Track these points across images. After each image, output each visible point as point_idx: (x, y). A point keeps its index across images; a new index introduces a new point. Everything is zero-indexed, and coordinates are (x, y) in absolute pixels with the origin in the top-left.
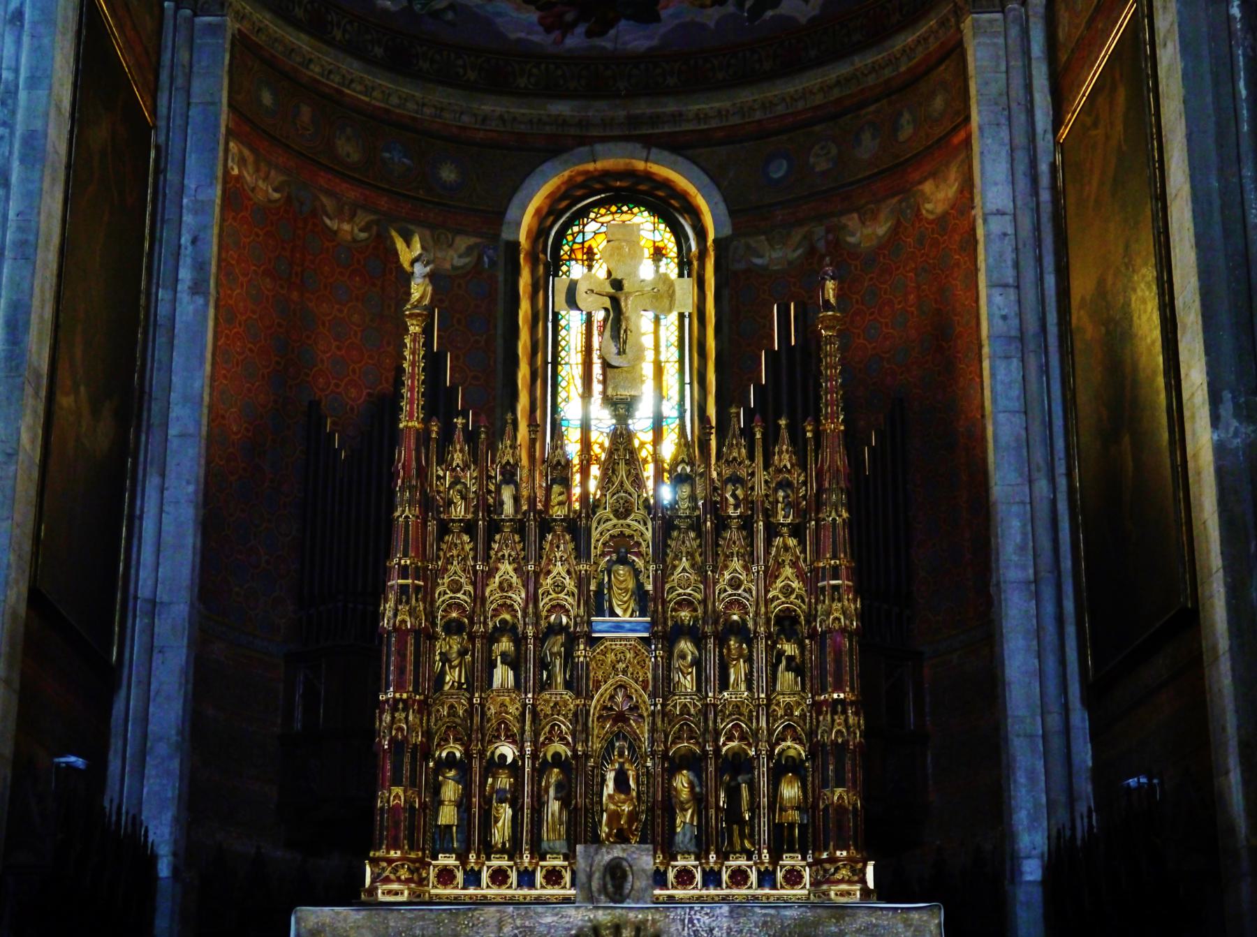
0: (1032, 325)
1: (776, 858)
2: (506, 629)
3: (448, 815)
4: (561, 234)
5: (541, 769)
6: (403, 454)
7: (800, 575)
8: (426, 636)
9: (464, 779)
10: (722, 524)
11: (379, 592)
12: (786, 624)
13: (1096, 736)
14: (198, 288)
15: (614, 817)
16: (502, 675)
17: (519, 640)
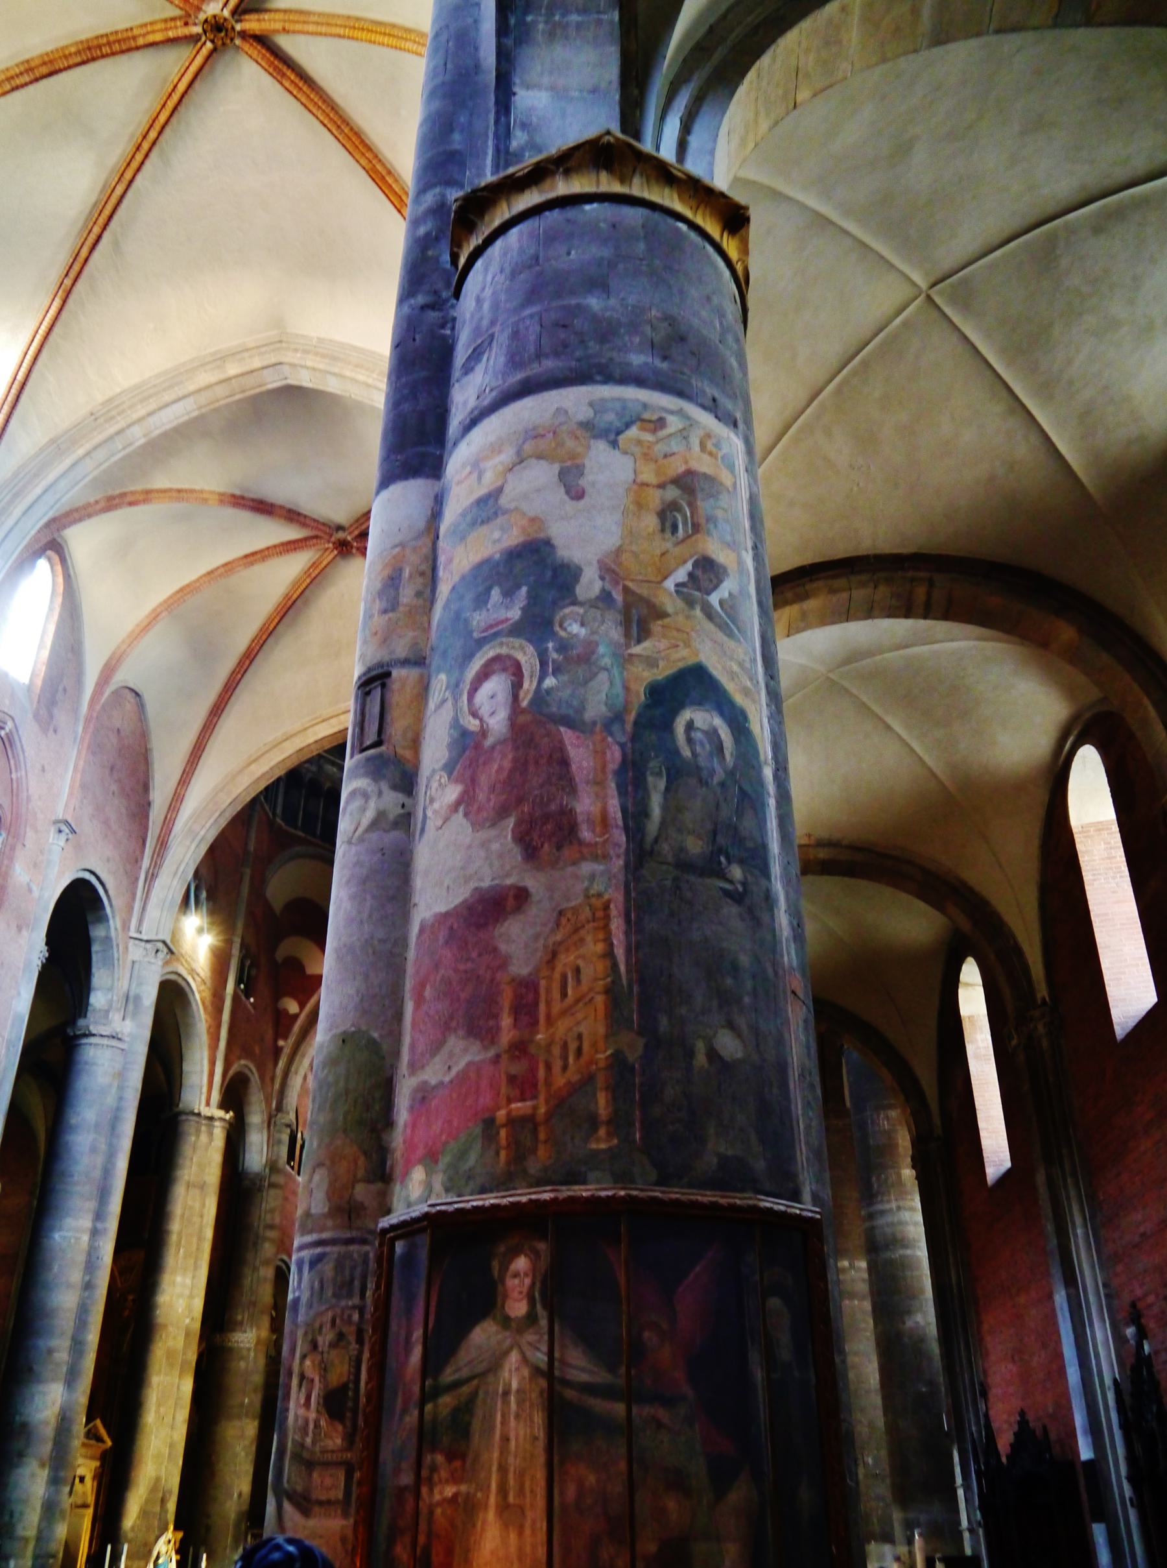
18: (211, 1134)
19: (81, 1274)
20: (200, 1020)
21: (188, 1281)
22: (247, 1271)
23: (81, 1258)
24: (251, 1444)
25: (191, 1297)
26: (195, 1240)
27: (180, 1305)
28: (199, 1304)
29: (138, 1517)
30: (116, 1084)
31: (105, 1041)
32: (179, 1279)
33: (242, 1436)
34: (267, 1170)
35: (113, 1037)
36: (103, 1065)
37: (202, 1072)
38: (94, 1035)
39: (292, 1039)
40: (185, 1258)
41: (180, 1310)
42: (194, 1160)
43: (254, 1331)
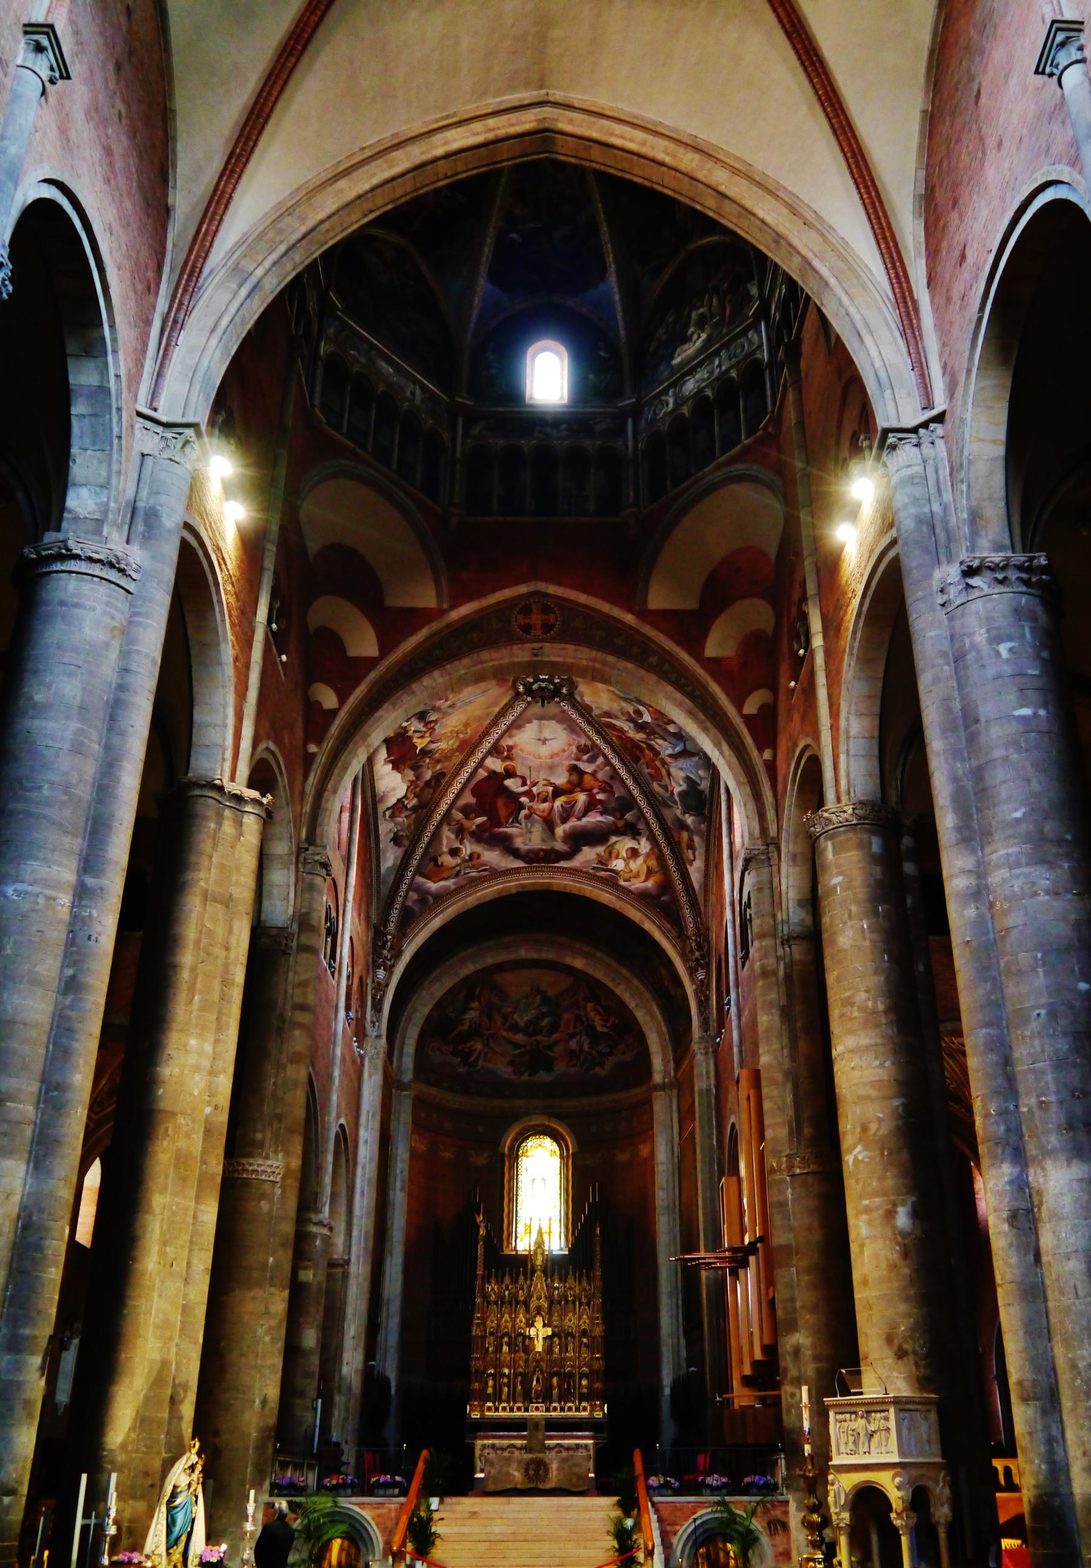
0: (671, 1205)
1: (580, 1403)
2: (506, 1334)
3: (490, 1390)
4: (519, 1147)
5: (516, 1375)
6: (478, 1282)
7: (588, 1318)
8: (484, 1337)
9: (494, 1380)
10: (567, 1302)
11: (471, 1324)
12: (584, 1333)
13: (687, 1346)
14: (402, 1189)
15: (536, 1391)
16: (505, 1348)
17: (510, 1338)
18: (239, 824)
19: (58, 964)
20: (226, 640)
21: (208, 1047)
22: (271, 1070)
23: (58, 935)
24: (281, 1322)
25: (213, 1073)
26: (217, 984)
27: (197, 1084)
28: (225, 1083)
29: (132, 1429)
30: (116, 644)
31: (96, 569)
32: (193, 1042)
33: (267, 1313)
34: (295, 926)
35: (112, 565)
36: (94, 609)
37: (225, 726)
38: (77, 557)
39: (329, 744)
40: (202, 1009)
41: (196, 1093)
42: (214, 860)
43: (280, 1156)
